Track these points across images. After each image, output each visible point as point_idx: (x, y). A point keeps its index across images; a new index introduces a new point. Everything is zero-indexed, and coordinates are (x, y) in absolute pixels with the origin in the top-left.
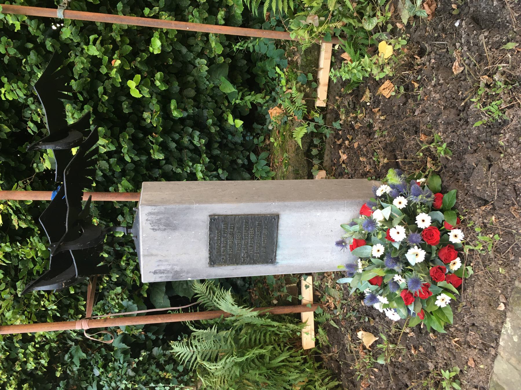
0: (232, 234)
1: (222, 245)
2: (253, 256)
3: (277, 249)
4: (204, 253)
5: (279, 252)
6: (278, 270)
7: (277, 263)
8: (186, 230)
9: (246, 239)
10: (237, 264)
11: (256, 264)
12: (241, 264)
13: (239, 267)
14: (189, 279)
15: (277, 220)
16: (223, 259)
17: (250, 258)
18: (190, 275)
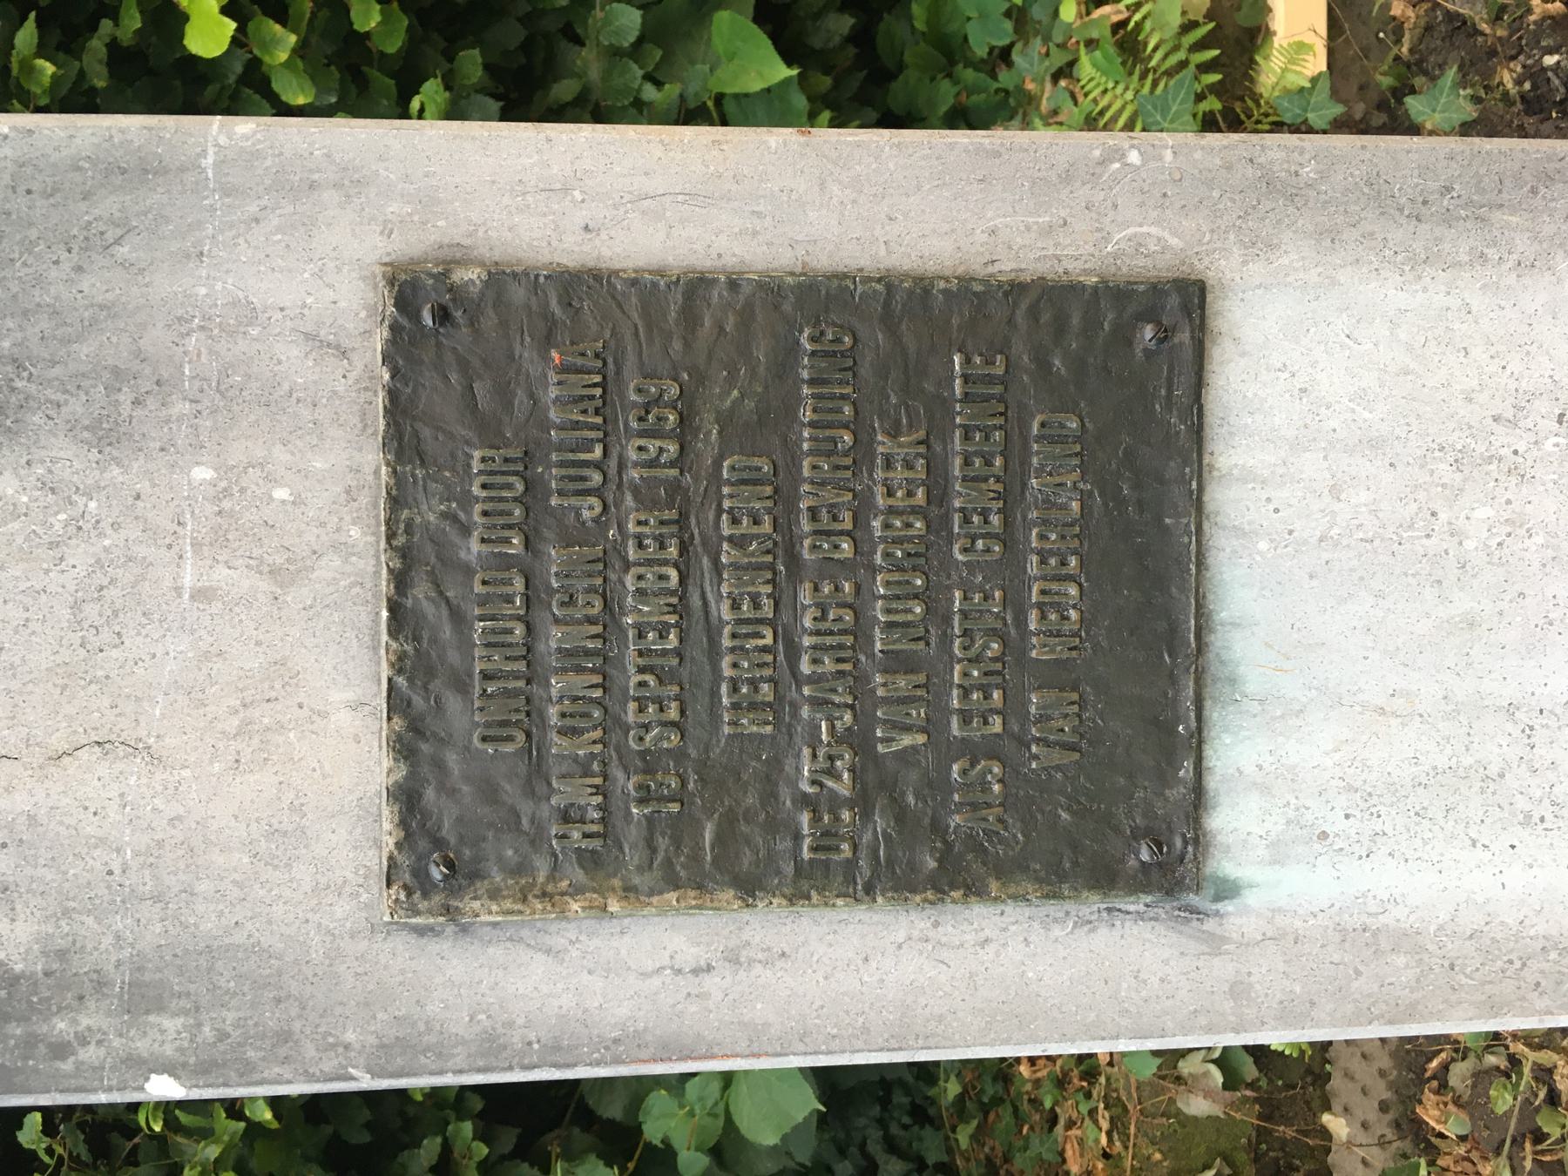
0: (678, 506)
1: (554, 638)
2: (937, 785)
3: (1213, 714)
4: (343, 754)
5: (1237, 753)
6: (1238, 990)
7: (1227, 890)
8: (106, 435)
9: (831, 568)
10: (750, 888)
11: (974, 890)
12: (797, 897)
13: (770, 927)
14: (163, 1088)
15: (1184, 337)
16: (565, 817)
17: (901, 816)
18: (167, 1031)
